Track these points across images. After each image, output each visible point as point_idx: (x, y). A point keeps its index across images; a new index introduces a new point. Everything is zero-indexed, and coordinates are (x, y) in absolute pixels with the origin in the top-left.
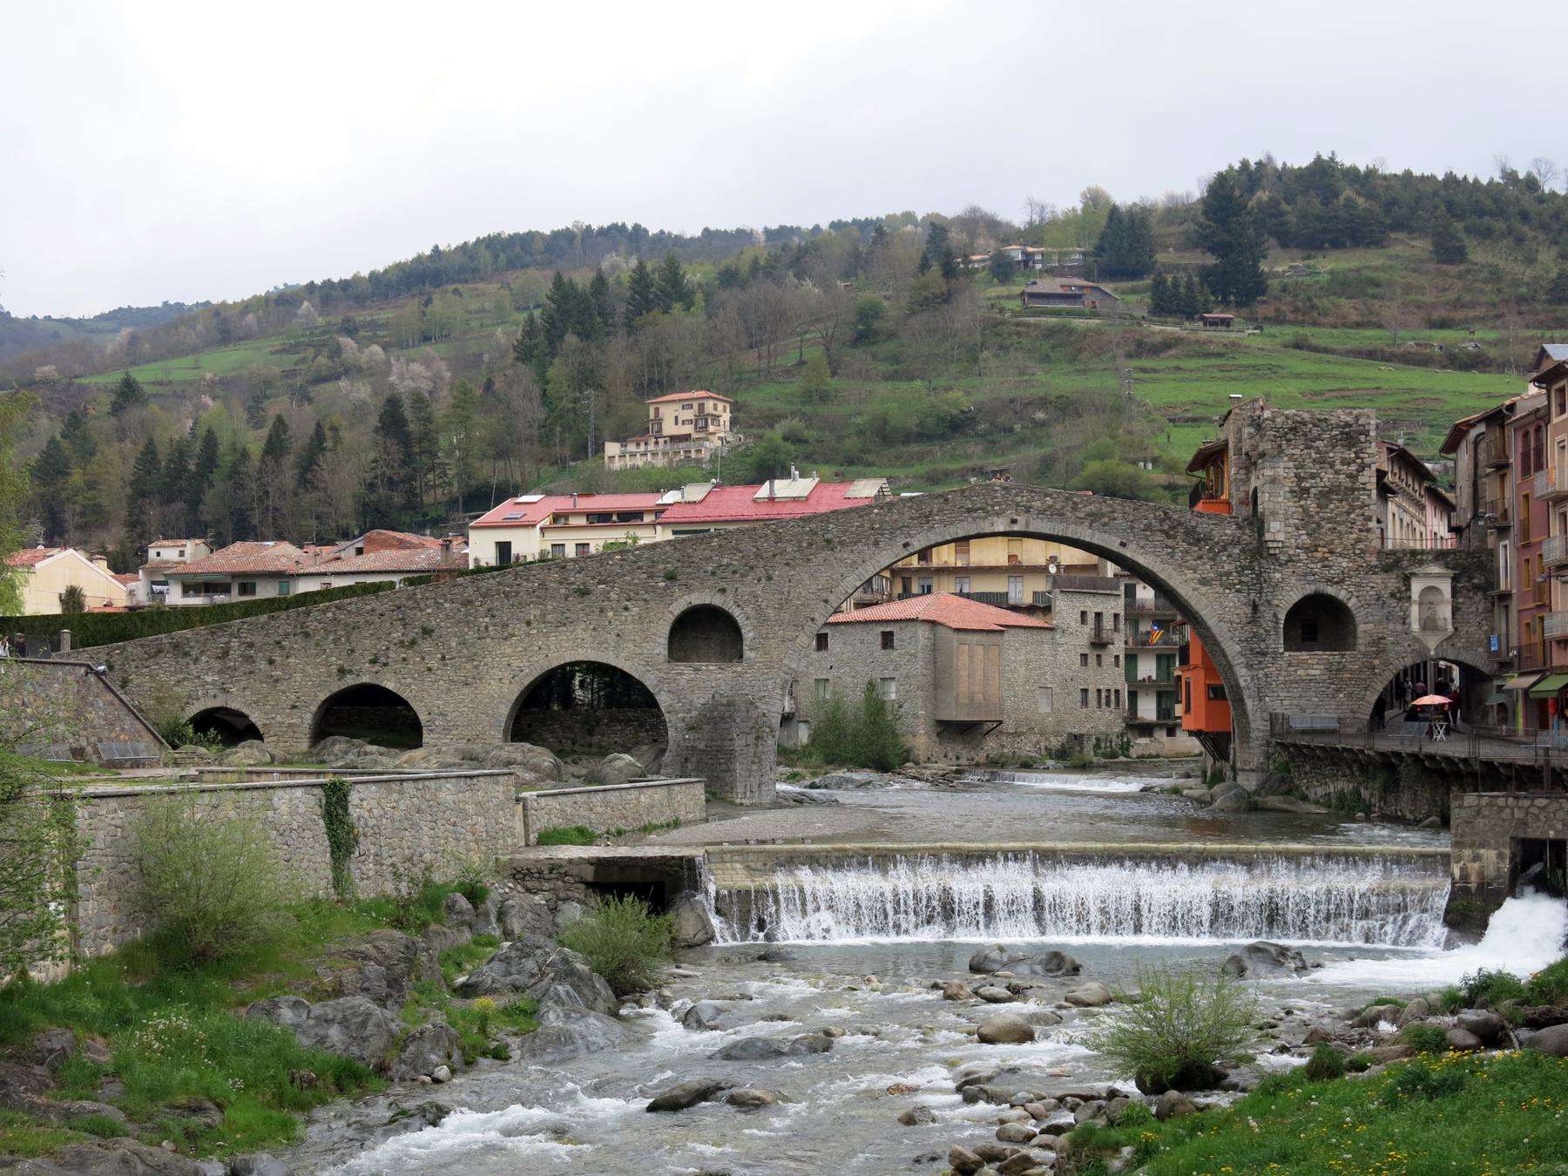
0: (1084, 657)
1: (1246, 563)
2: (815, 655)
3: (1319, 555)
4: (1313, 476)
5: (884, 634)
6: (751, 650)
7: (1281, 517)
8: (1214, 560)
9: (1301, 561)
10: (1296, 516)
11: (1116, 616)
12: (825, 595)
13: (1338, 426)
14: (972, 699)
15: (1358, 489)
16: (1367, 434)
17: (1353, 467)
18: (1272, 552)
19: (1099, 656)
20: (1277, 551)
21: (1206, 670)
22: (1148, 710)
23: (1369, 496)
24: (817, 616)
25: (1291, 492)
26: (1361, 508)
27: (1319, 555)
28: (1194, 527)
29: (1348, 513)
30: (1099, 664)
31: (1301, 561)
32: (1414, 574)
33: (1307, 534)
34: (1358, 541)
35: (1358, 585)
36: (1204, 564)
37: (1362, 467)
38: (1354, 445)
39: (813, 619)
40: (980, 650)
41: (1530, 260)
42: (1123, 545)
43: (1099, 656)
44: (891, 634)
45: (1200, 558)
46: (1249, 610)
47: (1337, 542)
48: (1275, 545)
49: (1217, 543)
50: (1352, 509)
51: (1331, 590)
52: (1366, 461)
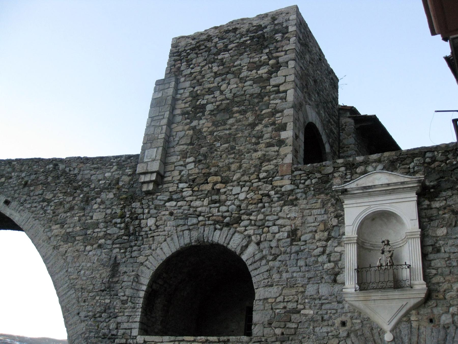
1: (118, 211)
3: (208, 187)
4: (210, 91)
7: (160, 143)
8: (84, 209)
9: (183, 198)
10: (183, 141)
13: (248, 31)
15: (268, 94)
16: (285, 31)
17: (263, 71)
18: (145, 188)
20: (151, 187)
23: (284, 99)
25: (183, 114)
26: (273, 114)
27: (208, 187)
28: (75, 175)
29: (253, 125)
31: (183, 198)
32: (345, 192)
33: (197, 162)
34: (265, 159)
35: (262, 225)
36: (73, 216)
37: (277, 67)
38: (266, 47)
45: (71, 208)
46: (106, 273)
47: (233, 167)
48: (148, 178)
49: (94, 188)
50: (259, 119)
52: (281, 60)
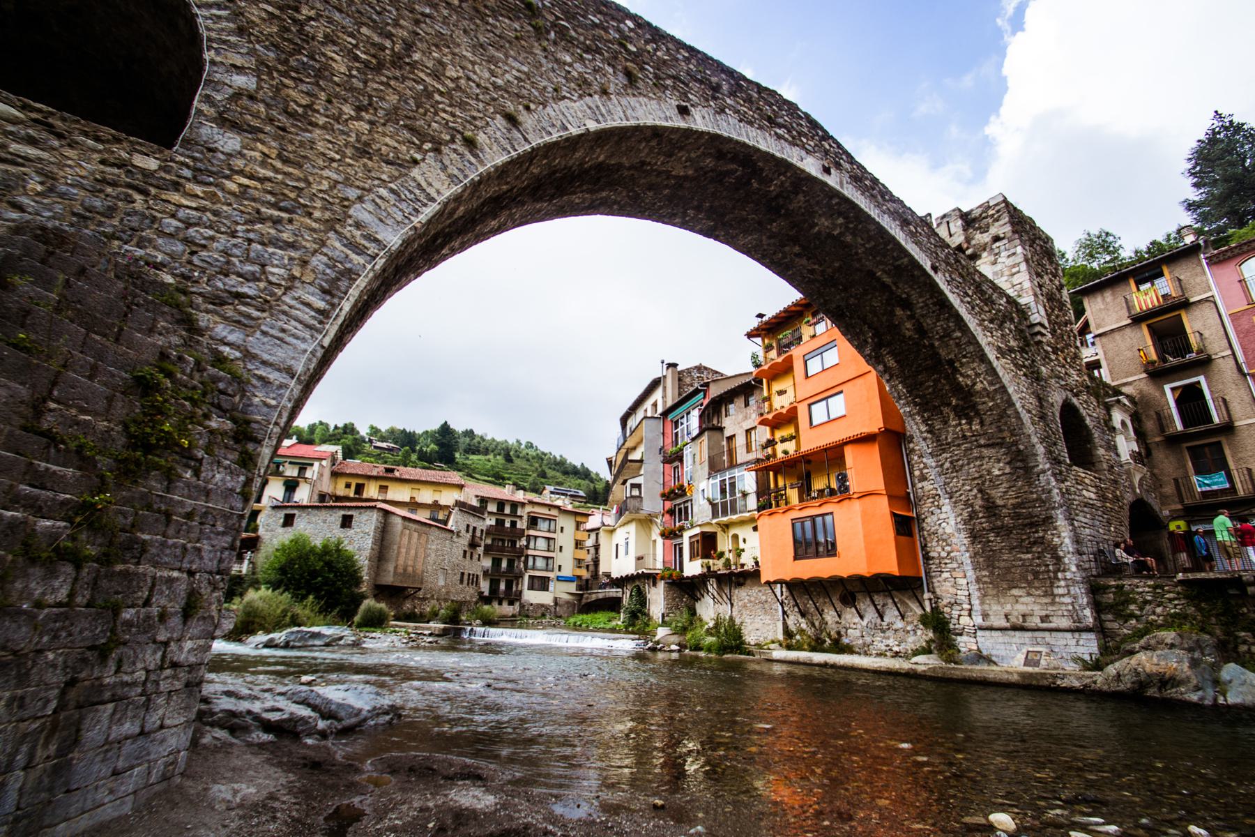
0: (465, 552)
2: (281, 530)
5: (344, 517)
6: (224, 121)
11: (482, 531)
12: (510, 107)
14: (405, 570)
19: (472, 553)
21: (891, 498)
22: (485, 586)
24: (481, 138)
30: (471, 558)
39: (470, 143)
40: (416, 535)
41: (531, 465)
42: (935, 269)
43: (472, 553)
44: (351, 517)
51: (1075, 400)
